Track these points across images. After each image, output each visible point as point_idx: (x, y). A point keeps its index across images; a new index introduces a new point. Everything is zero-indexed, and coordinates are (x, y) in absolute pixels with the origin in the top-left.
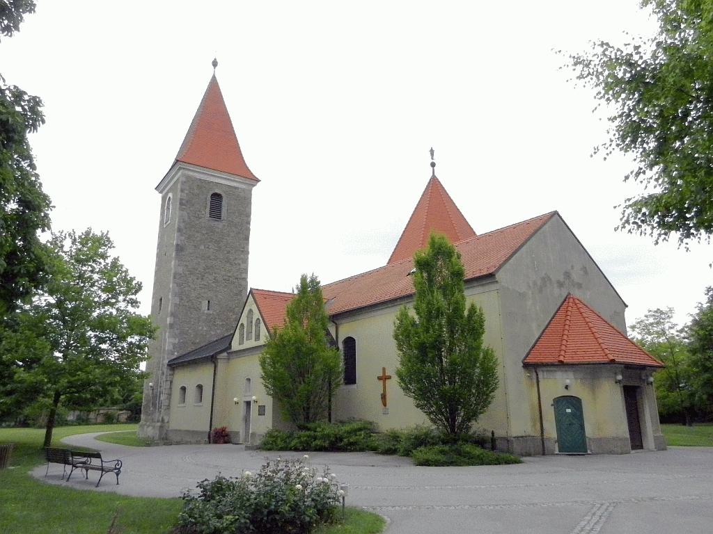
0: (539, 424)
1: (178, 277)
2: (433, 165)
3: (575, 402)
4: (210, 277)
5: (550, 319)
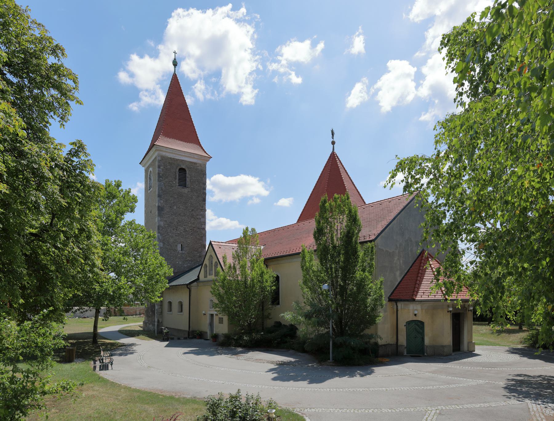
0: (395, 337)
1: (161, 229)
2: (333, 143)
3: (421, 324)
4: (182, 228)
5: (409, 268)
